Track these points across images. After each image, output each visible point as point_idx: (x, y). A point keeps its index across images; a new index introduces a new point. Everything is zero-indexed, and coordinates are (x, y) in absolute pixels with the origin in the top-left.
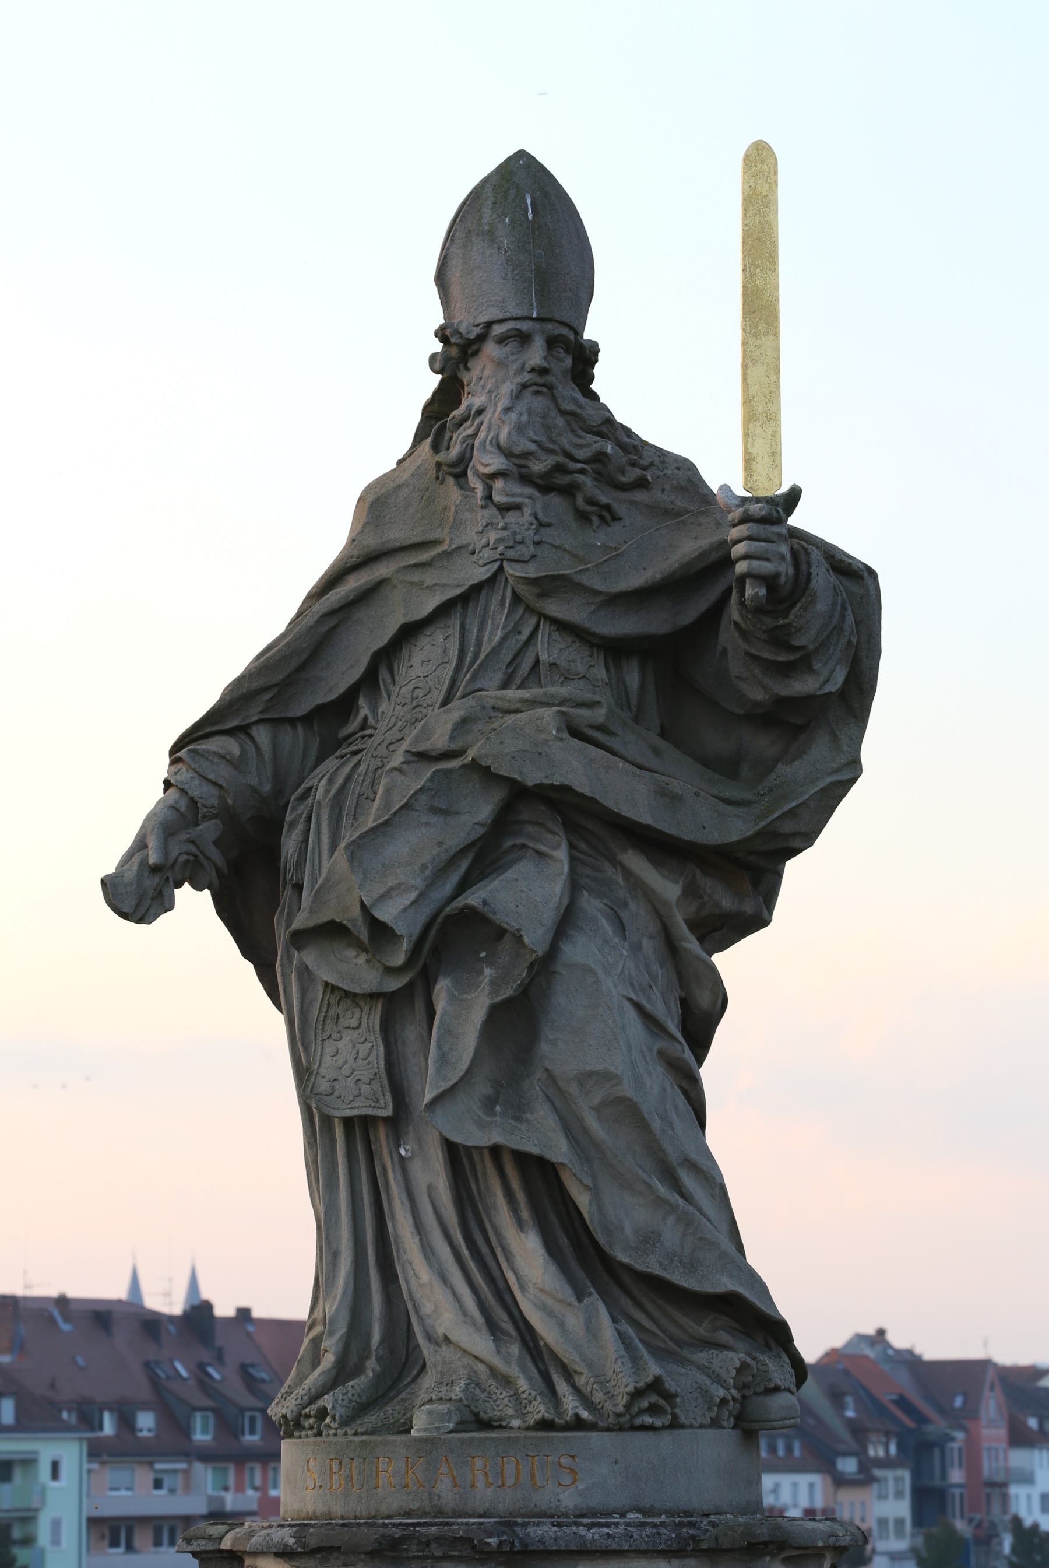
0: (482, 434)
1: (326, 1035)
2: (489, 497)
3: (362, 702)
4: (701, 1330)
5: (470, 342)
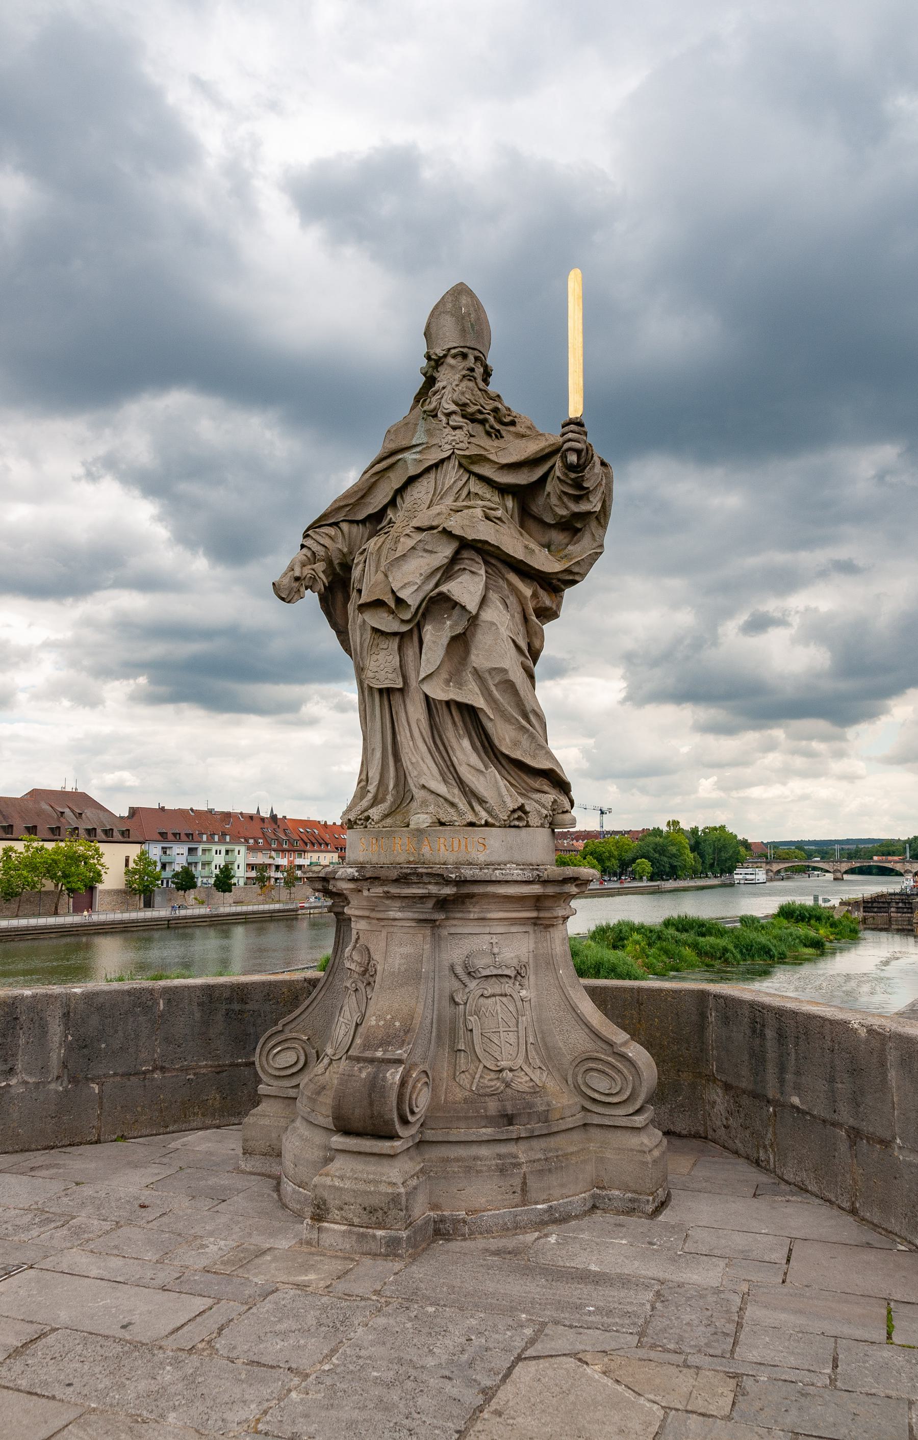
0: (445, 397)
1: (372, 652)
2: (448, 424)
3: (389, 512)
4: (537, 785)
5: (441, 358)
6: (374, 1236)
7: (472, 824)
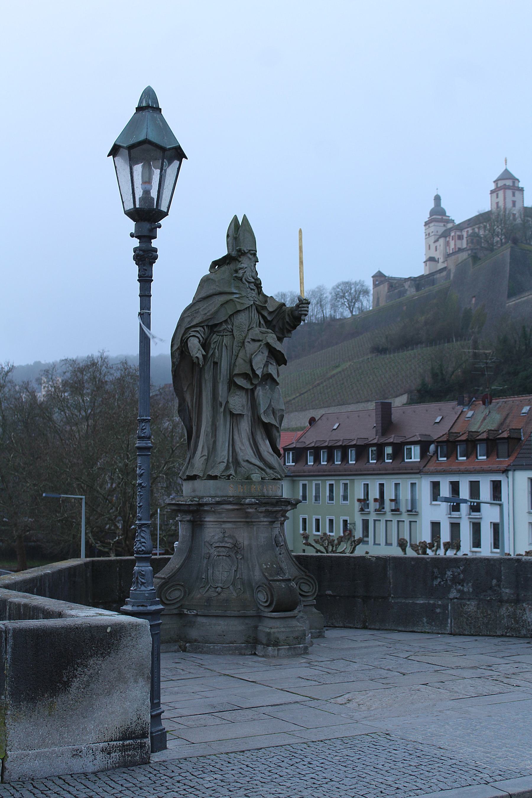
3: (224, 324)
5: (245, 253)
6: (299, 647)
7: (274, 479)
